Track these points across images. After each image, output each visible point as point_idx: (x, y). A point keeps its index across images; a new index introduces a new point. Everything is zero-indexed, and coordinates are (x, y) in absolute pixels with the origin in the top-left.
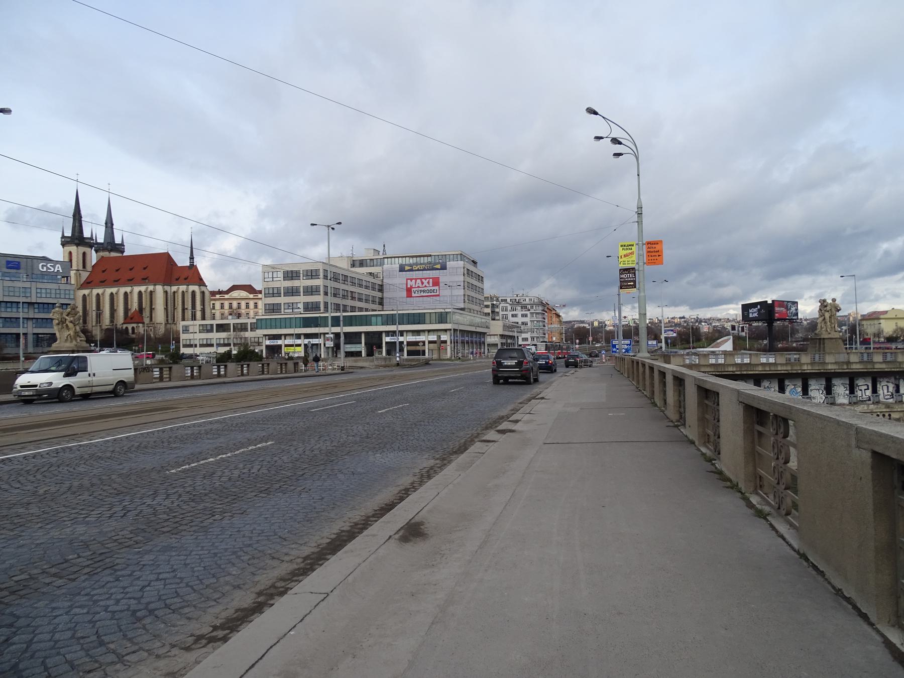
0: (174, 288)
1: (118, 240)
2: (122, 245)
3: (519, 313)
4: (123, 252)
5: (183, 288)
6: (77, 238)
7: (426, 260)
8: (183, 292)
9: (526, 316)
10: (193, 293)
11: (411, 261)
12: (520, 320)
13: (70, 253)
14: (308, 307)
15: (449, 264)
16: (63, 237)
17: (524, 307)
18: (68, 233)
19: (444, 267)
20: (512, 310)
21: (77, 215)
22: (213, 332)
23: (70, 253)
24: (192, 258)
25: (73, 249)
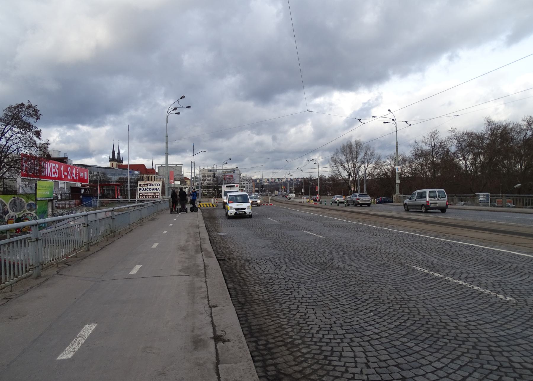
0: (149, 175)
1: (121, 159)
2: (122, 160)
3: (245, 183)
4: (123, 162)
5: (151, 175)
6: (112, 159)
7: (229, 171)
8: (151, 177)
9: (247, 183)
10: (154, 177)
11: (224, 171)
12: (245, 185)
13: (112, 164)
14: (208, 184)
15: (235, 172)
16: (110, 159)
17: (247, 181)
18: (111, 158)
19: (234, 173)
20: (243, 181)
21: (113, 152)
22: (224, 192)
23: (112, 164)
24: (153, 166)
25: (114, 163)
